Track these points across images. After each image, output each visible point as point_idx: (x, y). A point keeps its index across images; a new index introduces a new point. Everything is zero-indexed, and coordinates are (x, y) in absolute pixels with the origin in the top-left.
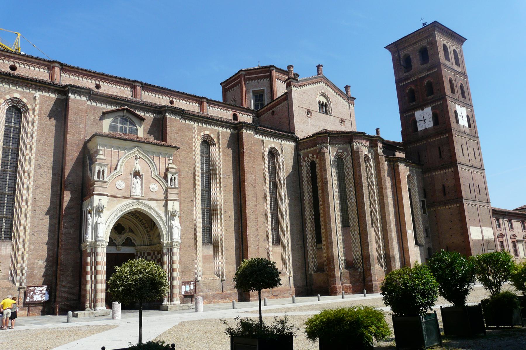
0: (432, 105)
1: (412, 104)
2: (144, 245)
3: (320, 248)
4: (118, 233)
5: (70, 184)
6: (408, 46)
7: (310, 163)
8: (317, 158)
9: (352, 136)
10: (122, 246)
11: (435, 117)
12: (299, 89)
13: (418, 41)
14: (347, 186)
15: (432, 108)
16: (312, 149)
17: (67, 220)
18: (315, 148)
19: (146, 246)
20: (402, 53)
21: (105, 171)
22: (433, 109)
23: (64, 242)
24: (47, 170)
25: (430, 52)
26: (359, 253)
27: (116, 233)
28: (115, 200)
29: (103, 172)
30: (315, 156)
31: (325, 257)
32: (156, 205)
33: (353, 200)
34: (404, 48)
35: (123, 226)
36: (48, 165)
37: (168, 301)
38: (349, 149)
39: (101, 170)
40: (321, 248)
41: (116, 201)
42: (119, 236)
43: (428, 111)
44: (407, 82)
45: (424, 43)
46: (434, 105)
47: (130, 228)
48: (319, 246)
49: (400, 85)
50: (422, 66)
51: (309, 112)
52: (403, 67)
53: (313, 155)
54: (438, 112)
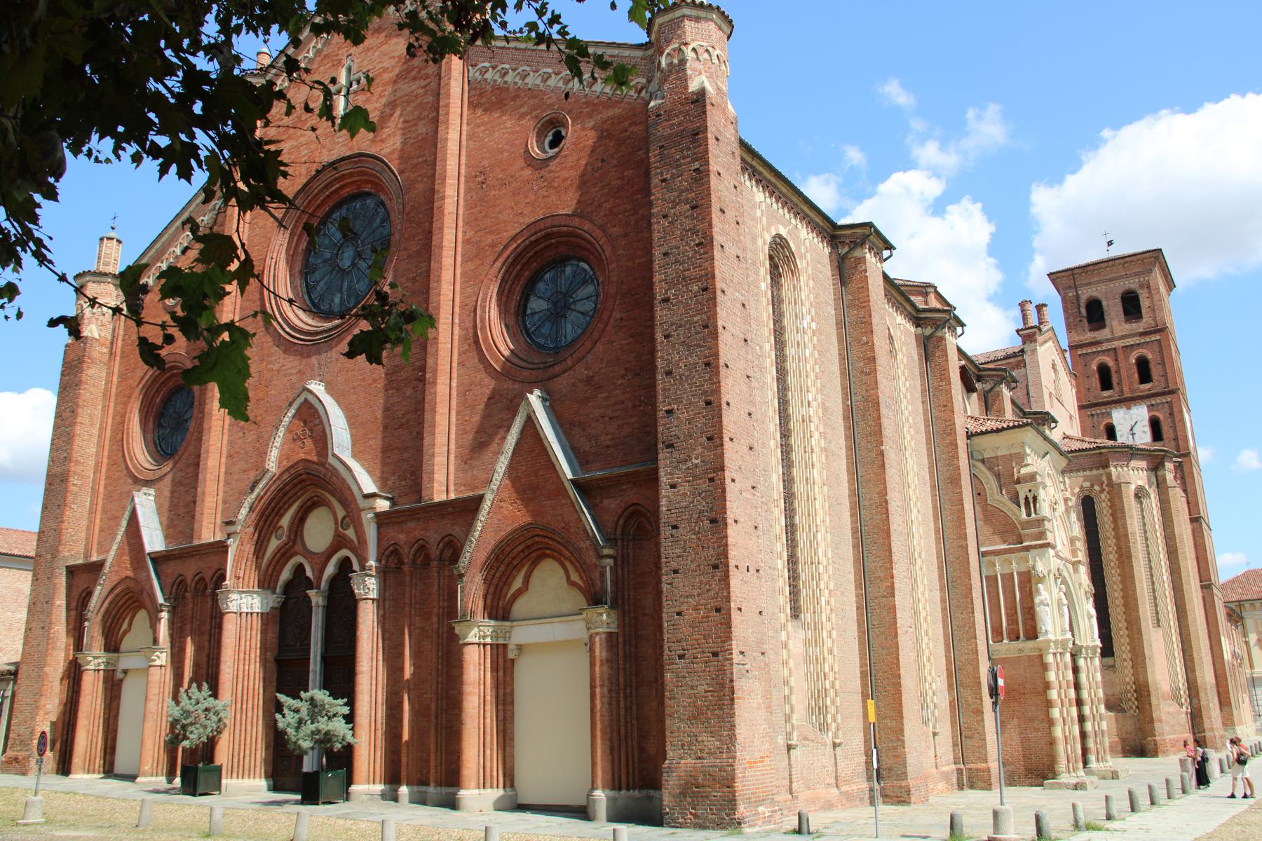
0: (1148, 403)
1: (1106, 393)
3: (1110, 667)
6: (1099, 282)
7: (1083, 500)
8: (1102, 491)
9: (1164, 456)
11: (1155, 425)
12: (1043, 348)
13: (1121, 277)
14: (1152, 549)
15: (1148, 407)
16: (1088, 473)
18: (1095, 472)
20: (1086, 294)
22: (1151, 407)
25: (1144, 303)
26: (1181, 677)
30: (1097, 488)
31: (1128, 683)
33: (1165, 578)
34: (1090, 284)
37: (1098, 760)
38: (1154, 480)
40: (1113, 666)
43: (1141, 413)
44: (1094, 350)
45: (1131, 284)
46: (1153, 402)
48: (1109, 661)
49: (1080, 353)
50: (1128, 326)
51: (1050, 394)
52: (1085, 320)
53: (1092, 486)
54: (1161, 417)
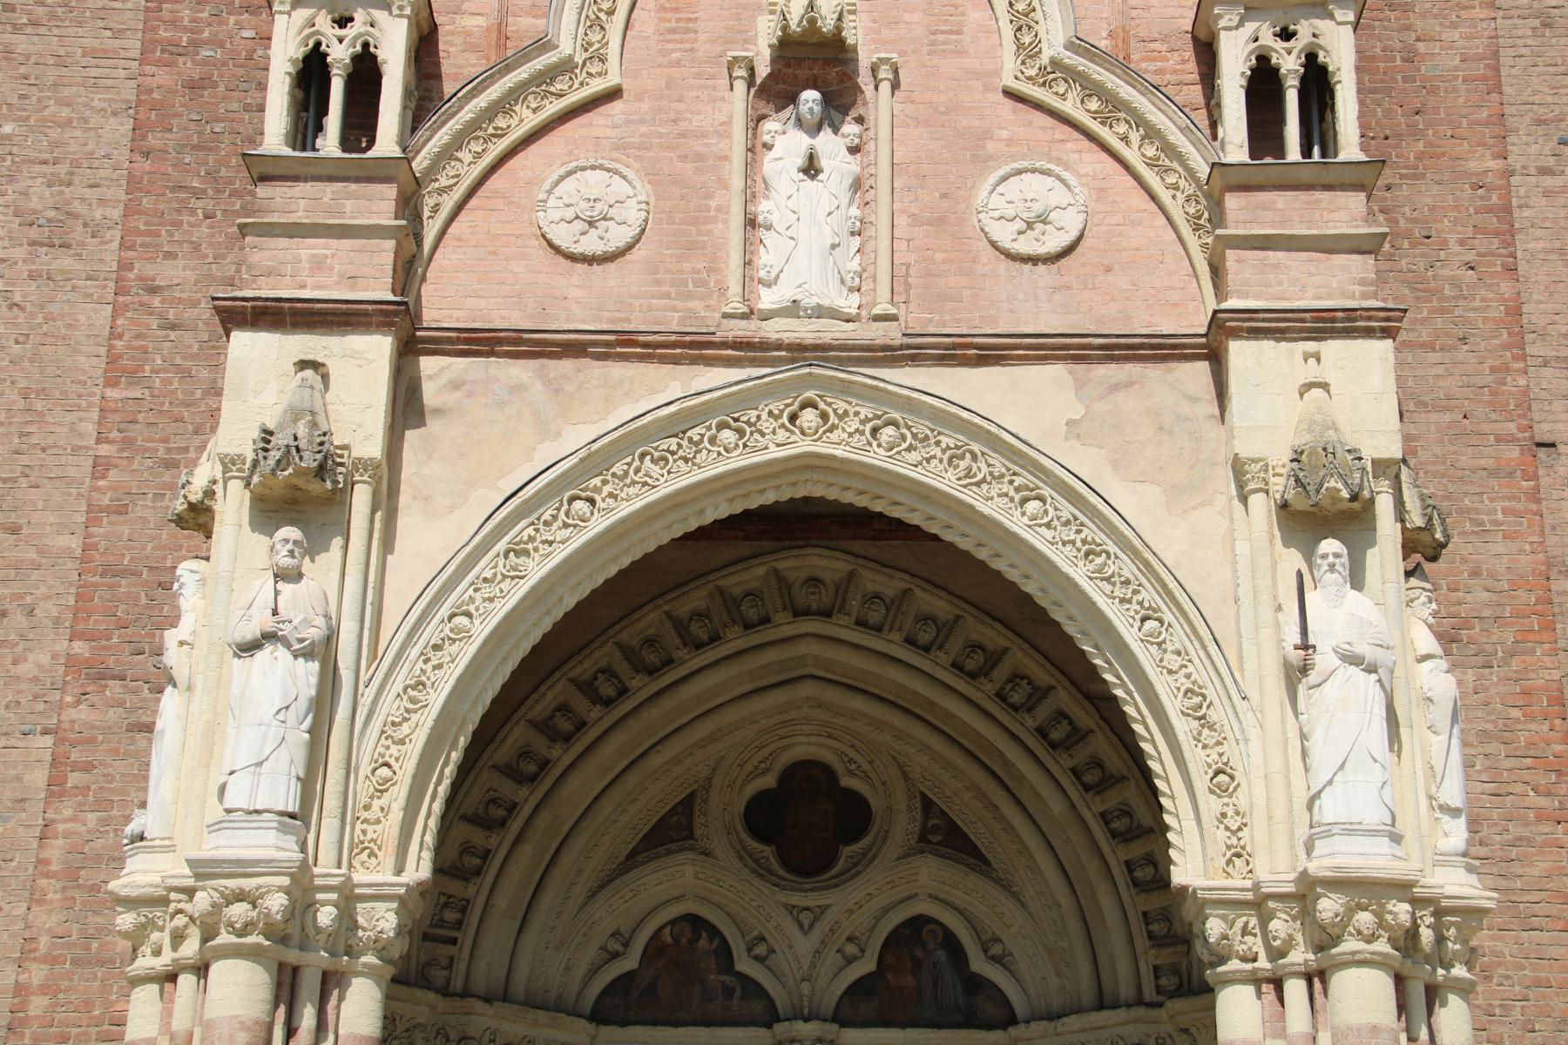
2: (1100, 1006)
4: (786, 864)
5: (173, 327)
10: (844, 1016)
17: (114, 715)
19: (1115, 1006)
21: (381, 54)
23: (51, 960)
24: (19, 253)
27: (760, 870)
28: (517, 389)
29: (366, 72)
32: (1078, 412)
35: (846, 781)
36: (34, 203)
39: (340, 55)
41: (538, 391)
42: (797, 899)
47: (927, 804)
